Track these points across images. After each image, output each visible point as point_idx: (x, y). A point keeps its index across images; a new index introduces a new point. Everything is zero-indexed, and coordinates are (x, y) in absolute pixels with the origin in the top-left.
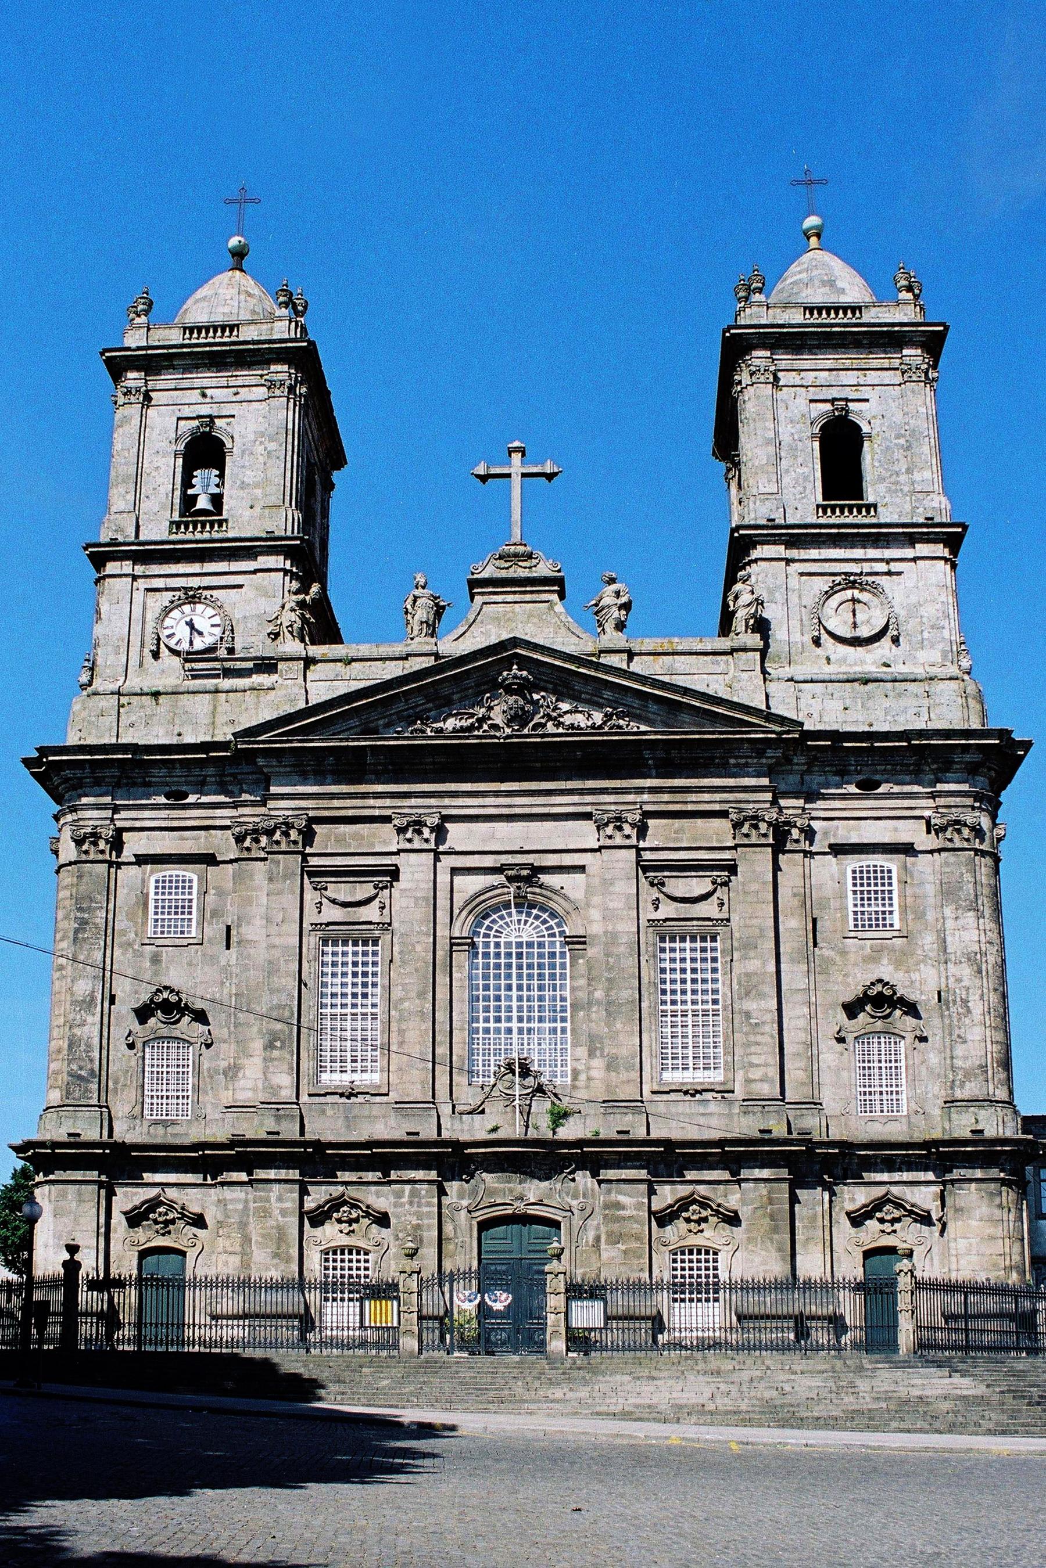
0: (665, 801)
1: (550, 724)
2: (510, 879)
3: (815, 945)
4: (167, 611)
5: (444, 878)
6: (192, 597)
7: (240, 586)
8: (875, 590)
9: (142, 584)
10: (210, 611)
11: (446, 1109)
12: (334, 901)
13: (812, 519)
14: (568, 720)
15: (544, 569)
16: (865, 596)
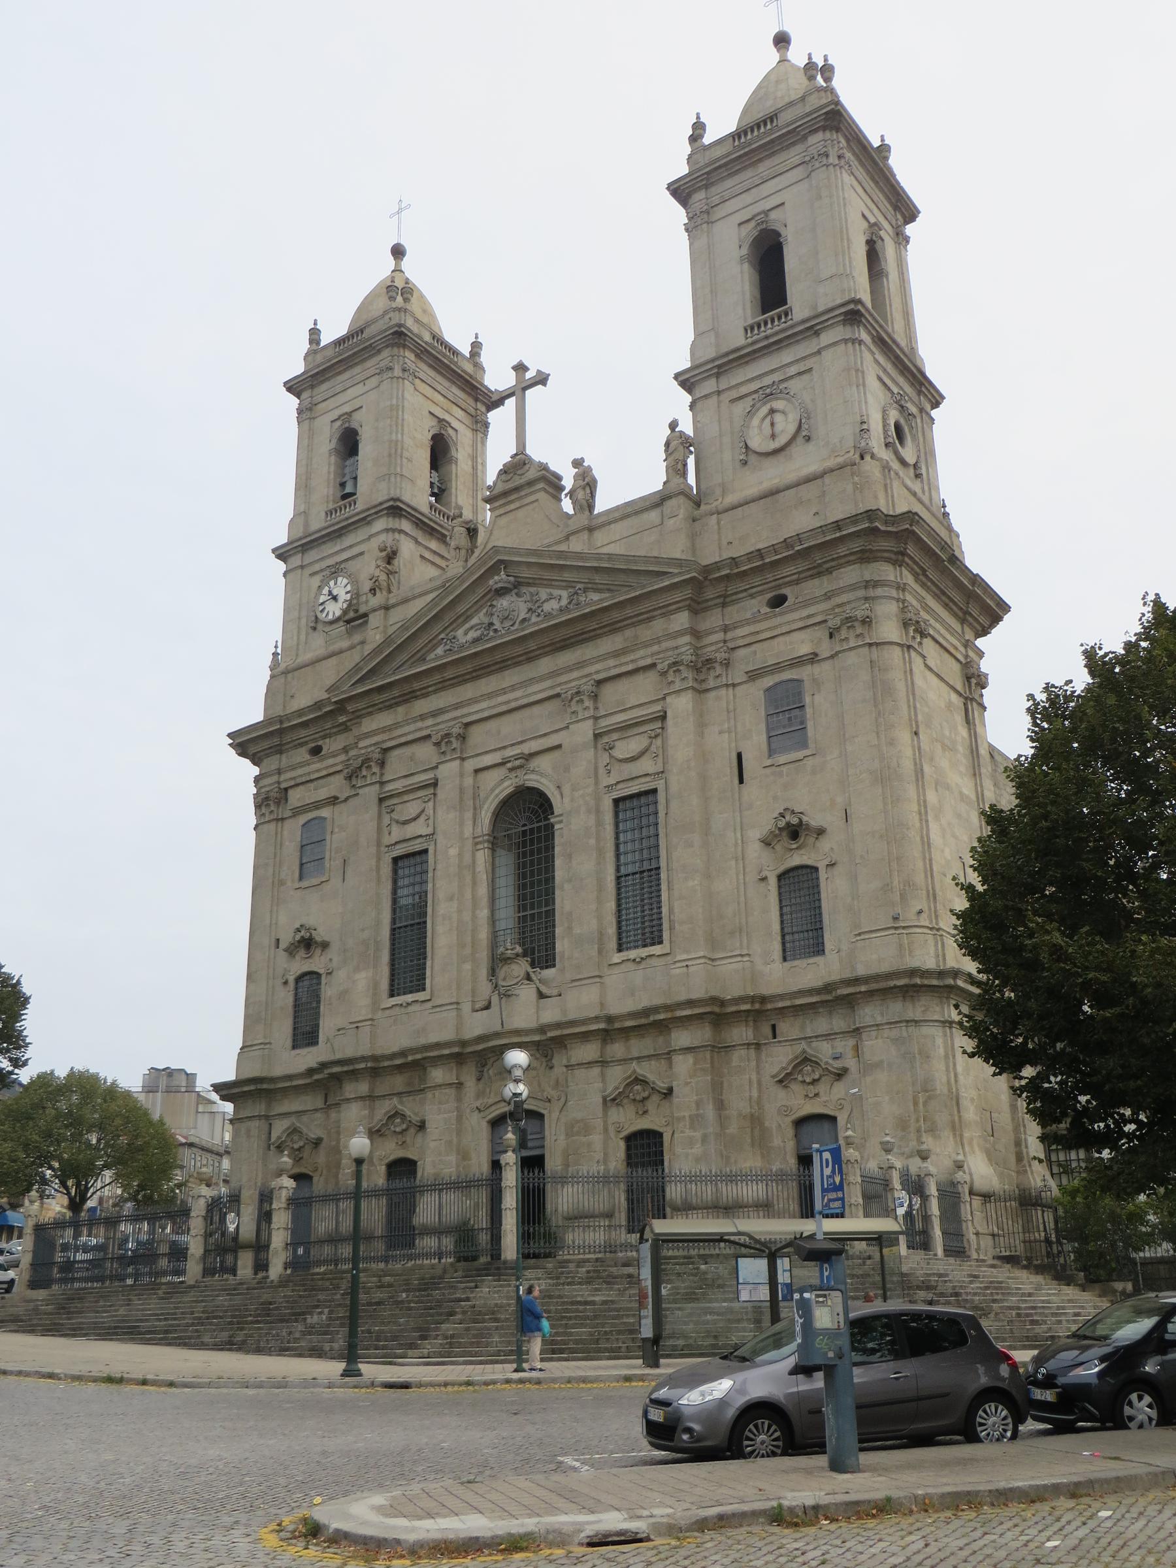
0: (612, 667)
1: (534, 619)
2: (511, 770)
3: (741, 781)
4: (320, 588)
5: (469, 781)
6: (335, 572)
7: (362, 554)
8: (786, 395)
9: (308, 571)
10: (345, 581)
11: (466, 1008)
12: (397, 822)
13: (741, 341)
14: (547, 607)
15: (532, 474)
16: (779, 404)
